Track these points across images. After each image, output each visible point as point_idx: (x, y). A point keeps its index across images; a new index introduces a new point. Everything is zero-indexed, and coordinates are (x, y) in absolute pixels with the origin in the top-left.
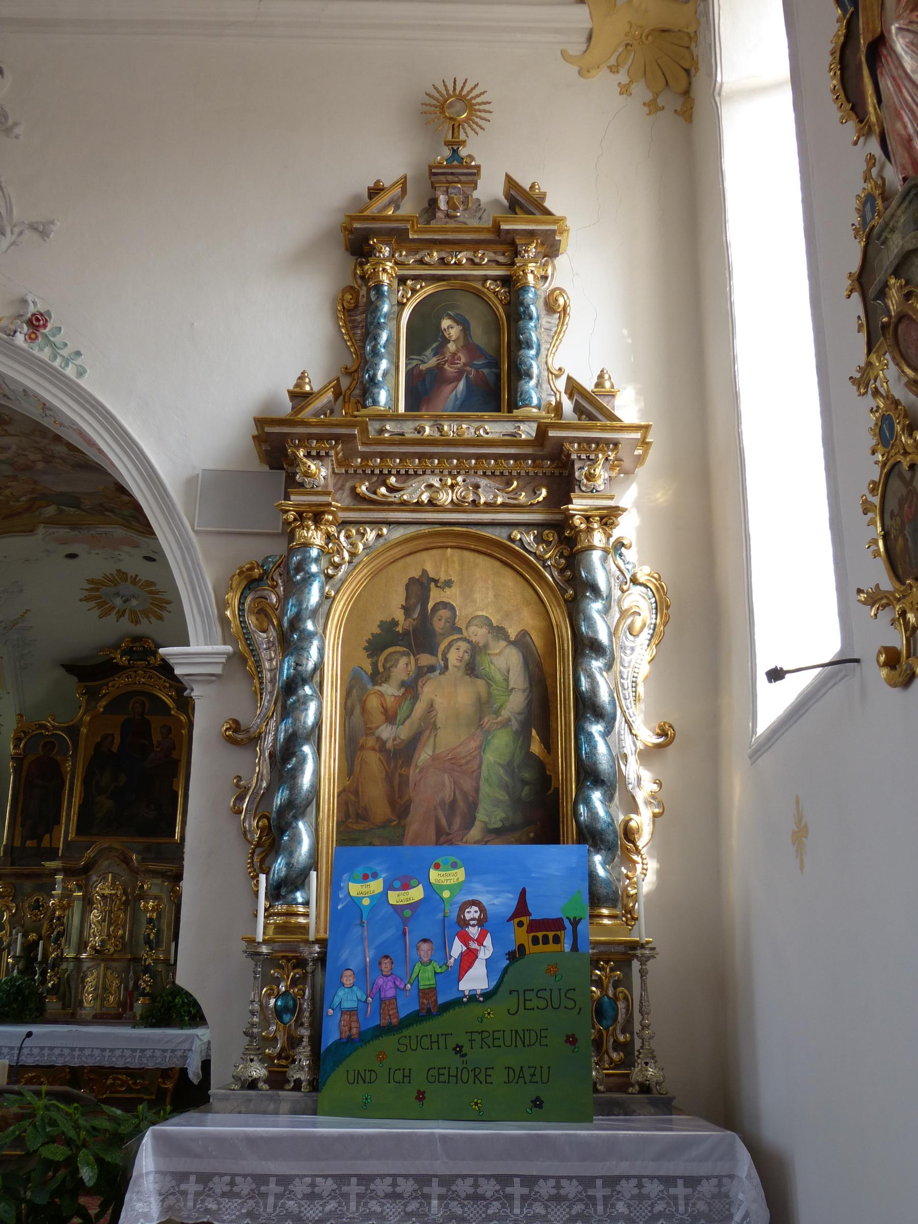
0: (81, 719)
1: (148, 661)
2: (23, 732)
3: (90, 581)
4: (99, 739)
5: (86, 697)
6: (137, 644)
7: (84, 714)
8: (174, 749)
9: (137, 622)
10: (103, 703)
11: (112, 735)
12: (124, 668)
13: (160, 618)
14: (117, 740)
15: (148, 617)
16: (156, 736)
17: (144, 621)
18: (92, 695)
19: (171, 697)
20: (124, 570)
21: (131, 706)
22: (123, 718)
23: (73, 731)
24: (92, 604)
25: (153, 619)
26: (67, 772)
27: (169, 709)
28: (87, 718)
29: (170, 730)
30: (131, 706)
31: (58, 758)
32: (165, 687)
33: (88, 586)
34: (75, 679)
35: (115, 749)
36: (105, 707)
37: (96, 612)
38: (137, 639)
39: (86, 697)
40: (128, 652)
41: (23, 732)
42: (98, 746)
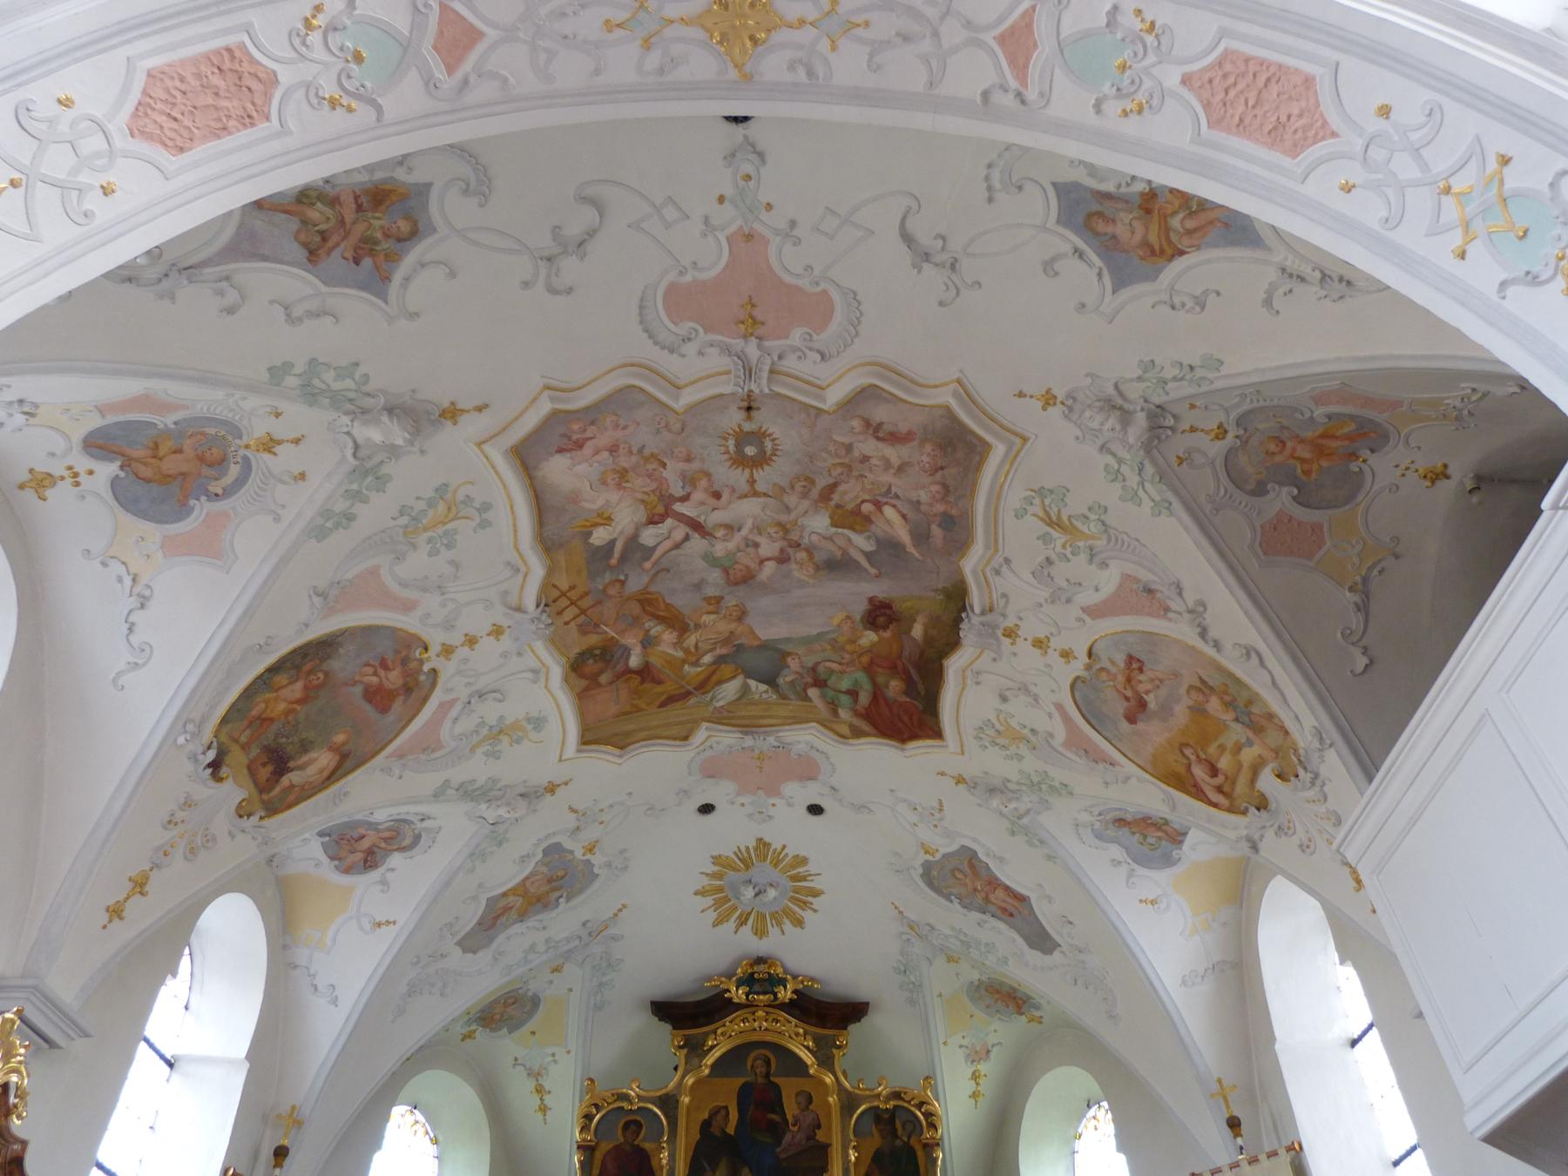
0: (680, 1084)
1: (775, 995)
2: (596, 1105)
3: (717, 860)
4: (706, 1116)
5: (685, 1051)
6: (762, 967)
7: (683, 1077)
8: (819, 1127)
9: (760, 932)
10: (710, 1060)
11: (726, 1107)
12: (739, 1007)
13: (799, 923)
14: (734, 1116)
15: (779, 924)
16: (791, 1108)
17: (774, 931)
18: (695, 1049)
19: (807, 1048)
20: (767, 840)
21: (749, 1064)
22: (741, 1081)
23: (668, 1103)
24: (709, 901)
25: (787, 925)
26: (662, 1168)
27: (806, 1066)
28: (690, 1080)
29: (810, 1099)
30: (749, 1064)
31: (647, 1146)
32: (797, 1034)
33: (712, 869)
34: (668, 1027)
35: (731, 1130)
36: (714, 1067)
37: (712, 915)
38: (760, 960)
39: (685, 1051)
40: (749, 981)
41: (596, 1105)
42: (706, 1125)
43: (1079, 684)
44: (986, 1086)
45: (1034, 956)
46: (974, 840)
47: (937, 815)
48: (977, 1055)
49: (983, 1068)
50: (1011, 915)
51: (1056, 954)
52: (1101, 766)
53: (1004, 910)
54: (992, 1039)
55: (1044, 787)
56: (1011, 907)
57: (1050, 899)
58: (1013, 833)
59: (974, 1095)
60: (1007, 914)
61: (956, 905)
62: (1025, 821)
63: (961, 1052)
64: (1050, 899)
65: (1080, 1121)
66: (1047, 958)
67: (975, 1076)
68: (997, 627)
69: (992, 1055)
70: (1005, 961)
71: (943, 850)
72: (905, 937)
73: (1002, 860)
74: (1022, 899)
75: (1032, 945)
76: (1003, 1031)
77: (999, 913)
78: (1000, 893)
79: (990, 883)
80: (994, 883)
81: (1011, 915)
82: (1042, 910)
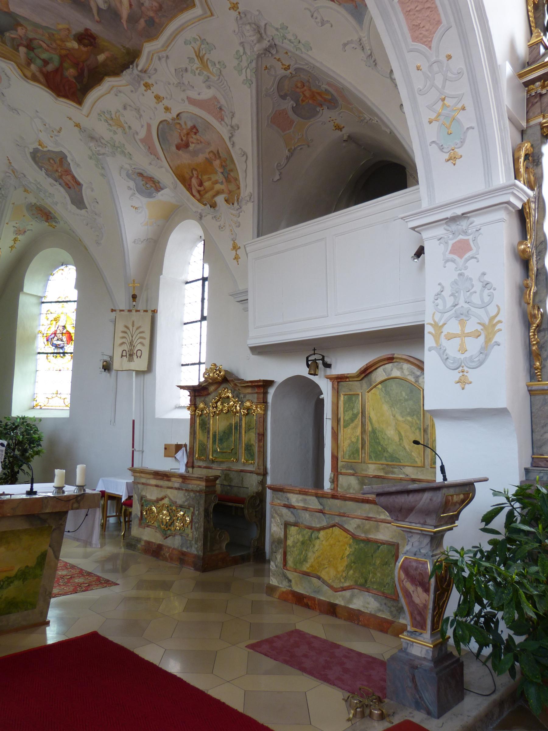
43: (164, 123)
44: (18, 245)
45: (73, 208)
46: (69, 152)
47: (55, 133)
48: (19, 232)
49: (20, 237)
50: (70, 188)
51: (83, 211)
52: (153, 157)
53: (67, 184)
54: (29, 227)
55: (119, 149)
56: (73, 186)
57: (92, 190)
58: (91, 158)
59: (12, 247)
60: (67, 187)
61: (43, 172)
62: (100, 157)
63: (13, 229)
64: (92, 190)
65: (55, 269)
66: (78, 211)
67: (15, 240)
68: (143, 80)
69: (26, 234)
70: (56, 204)
71: (49, 148)
72: (8, 174)
73: (78, 165)
74: (79, 184)
75: (73, 202)
76: (35, 226)
77: (63, 184)
78: (69, 178)
79: (66, 171)
80: (68, 172)
81: (70, 188)
82: (86, 193)
